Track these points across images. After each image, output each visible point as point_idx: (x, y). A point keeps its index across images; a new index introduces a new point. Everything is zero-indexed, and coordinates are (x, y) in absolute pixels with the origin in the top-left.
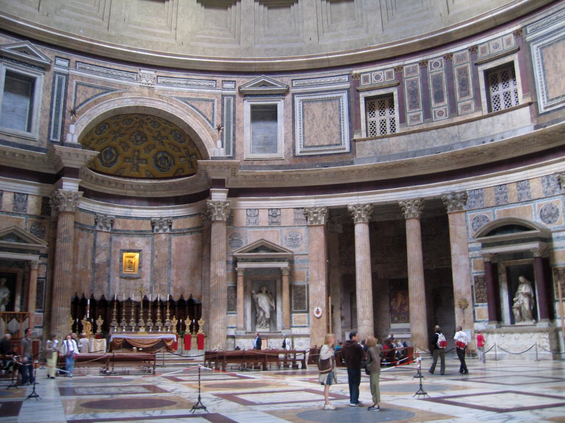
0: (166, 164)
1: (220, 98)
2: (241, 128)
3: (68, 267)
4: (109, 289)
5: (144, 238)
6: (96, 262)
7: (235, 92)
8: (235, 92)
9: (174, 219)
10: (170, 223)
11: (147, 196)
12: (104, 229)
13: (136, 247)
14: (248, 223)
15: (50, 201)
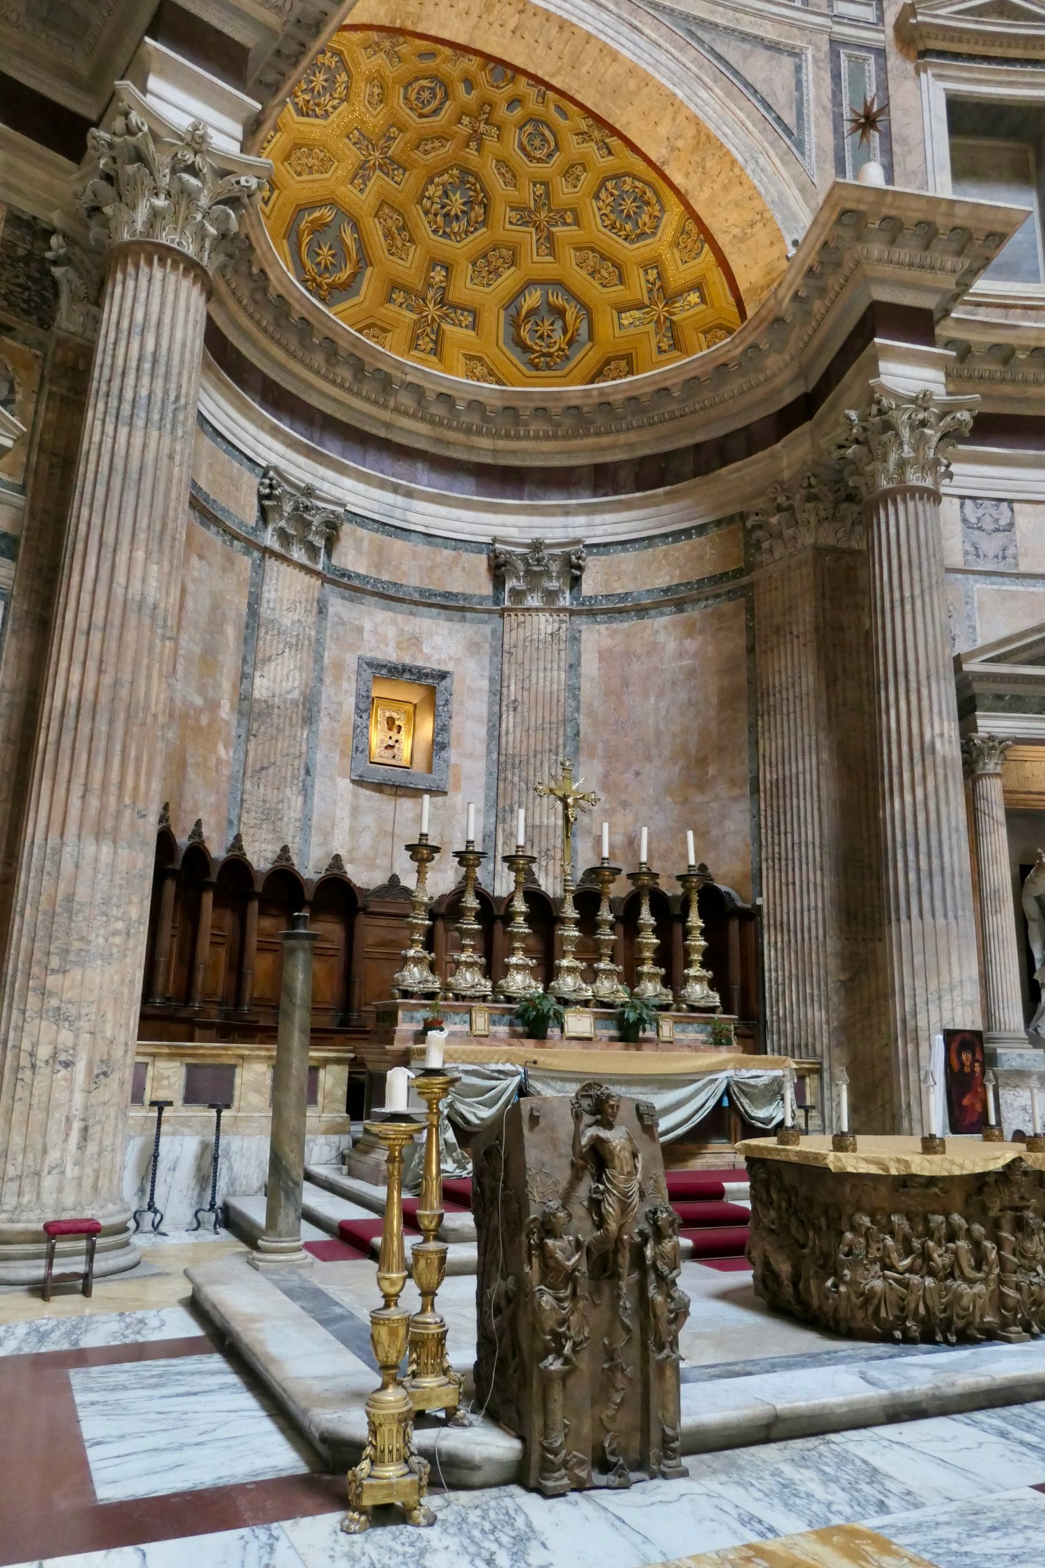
0: (558, 335)
1: (826, 47)
2: (914, 173)
3: (153, 583)
4: (305, 824)
5: (457, 626)
6: (257, 694)
7: (881, 37)
8: (886, 37)
9: (590, 554)
10: (579, 568)
11: (475, 458)
12: (298, 554)
13: (428, 658)
14: (971, 558)
15: (54, 241)
